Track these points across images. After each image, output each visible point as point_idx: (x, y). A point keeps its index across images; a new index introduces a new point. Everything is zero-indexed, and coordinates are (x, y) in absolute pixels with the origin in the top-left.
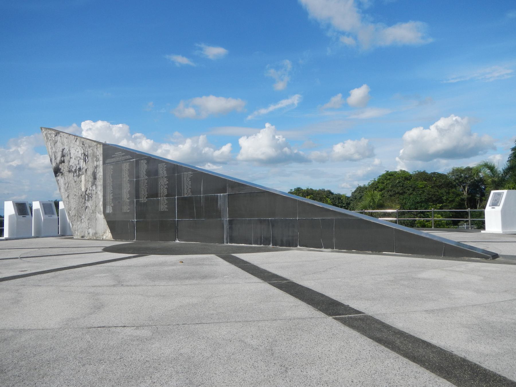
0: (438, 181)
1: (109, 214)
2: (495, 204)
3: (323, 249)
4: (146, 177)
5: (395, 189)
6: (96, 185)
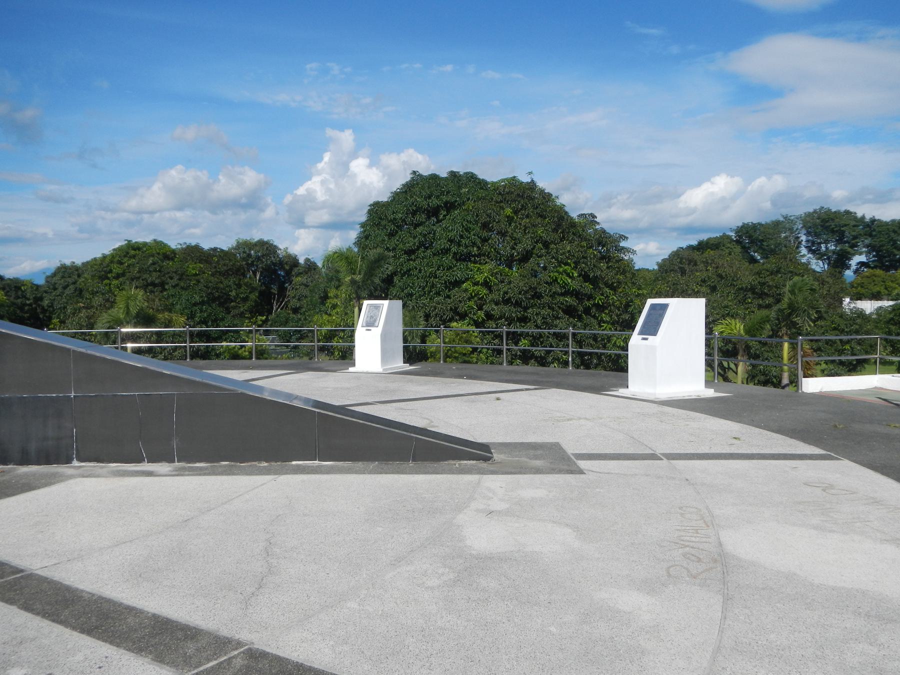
0: (222, 262)
2: (370, 324)
3: (146, 466)
5: (146, 276)
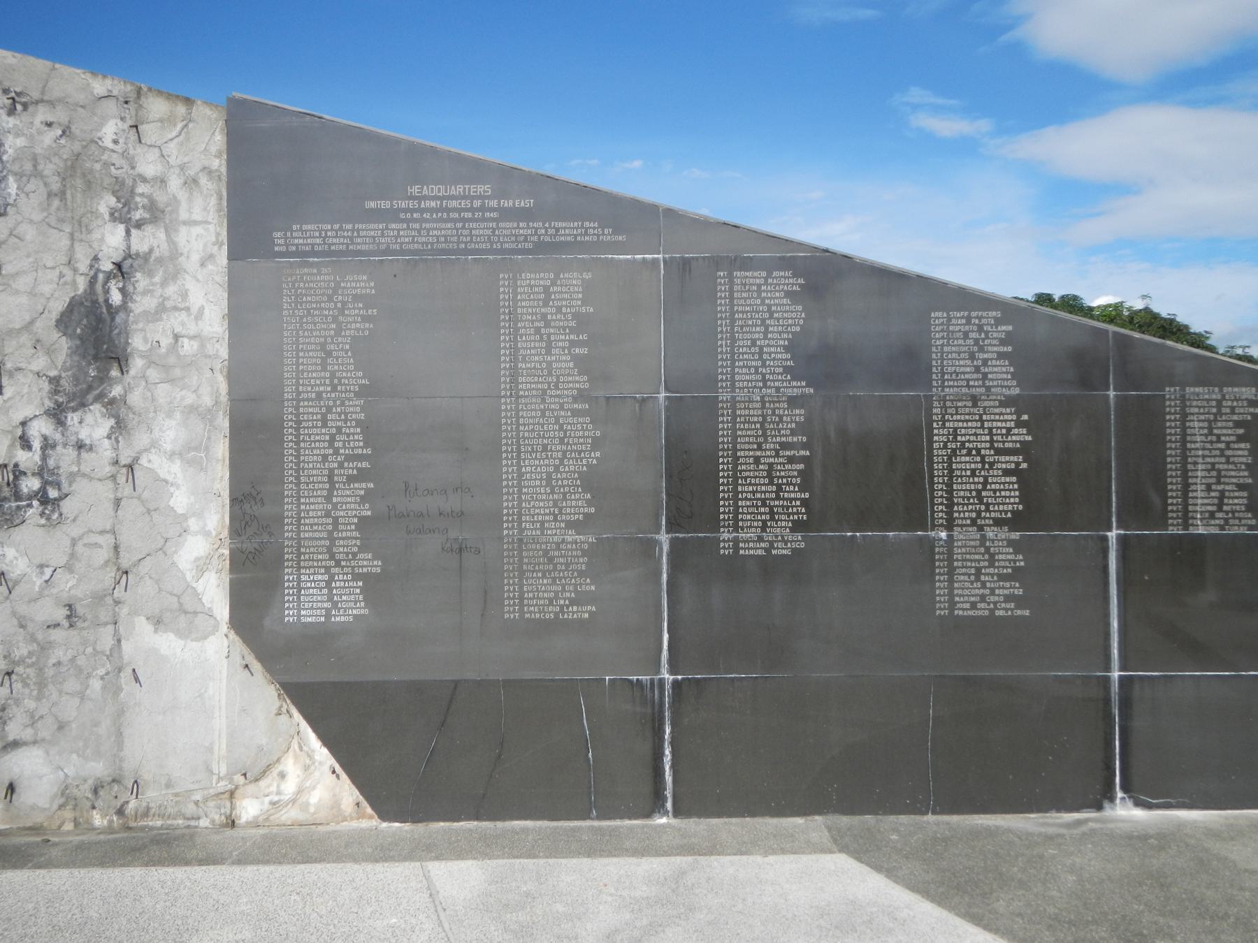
1: (319, 639)
4: (799, 388)
6: (113, 407)
